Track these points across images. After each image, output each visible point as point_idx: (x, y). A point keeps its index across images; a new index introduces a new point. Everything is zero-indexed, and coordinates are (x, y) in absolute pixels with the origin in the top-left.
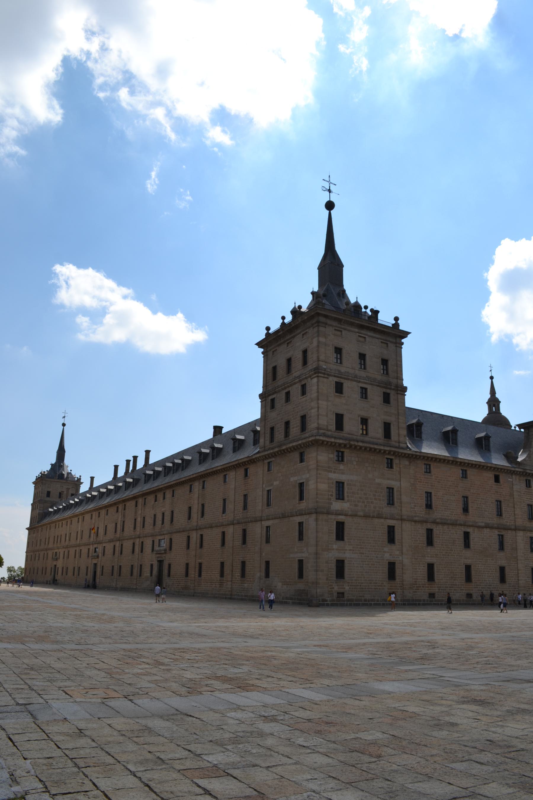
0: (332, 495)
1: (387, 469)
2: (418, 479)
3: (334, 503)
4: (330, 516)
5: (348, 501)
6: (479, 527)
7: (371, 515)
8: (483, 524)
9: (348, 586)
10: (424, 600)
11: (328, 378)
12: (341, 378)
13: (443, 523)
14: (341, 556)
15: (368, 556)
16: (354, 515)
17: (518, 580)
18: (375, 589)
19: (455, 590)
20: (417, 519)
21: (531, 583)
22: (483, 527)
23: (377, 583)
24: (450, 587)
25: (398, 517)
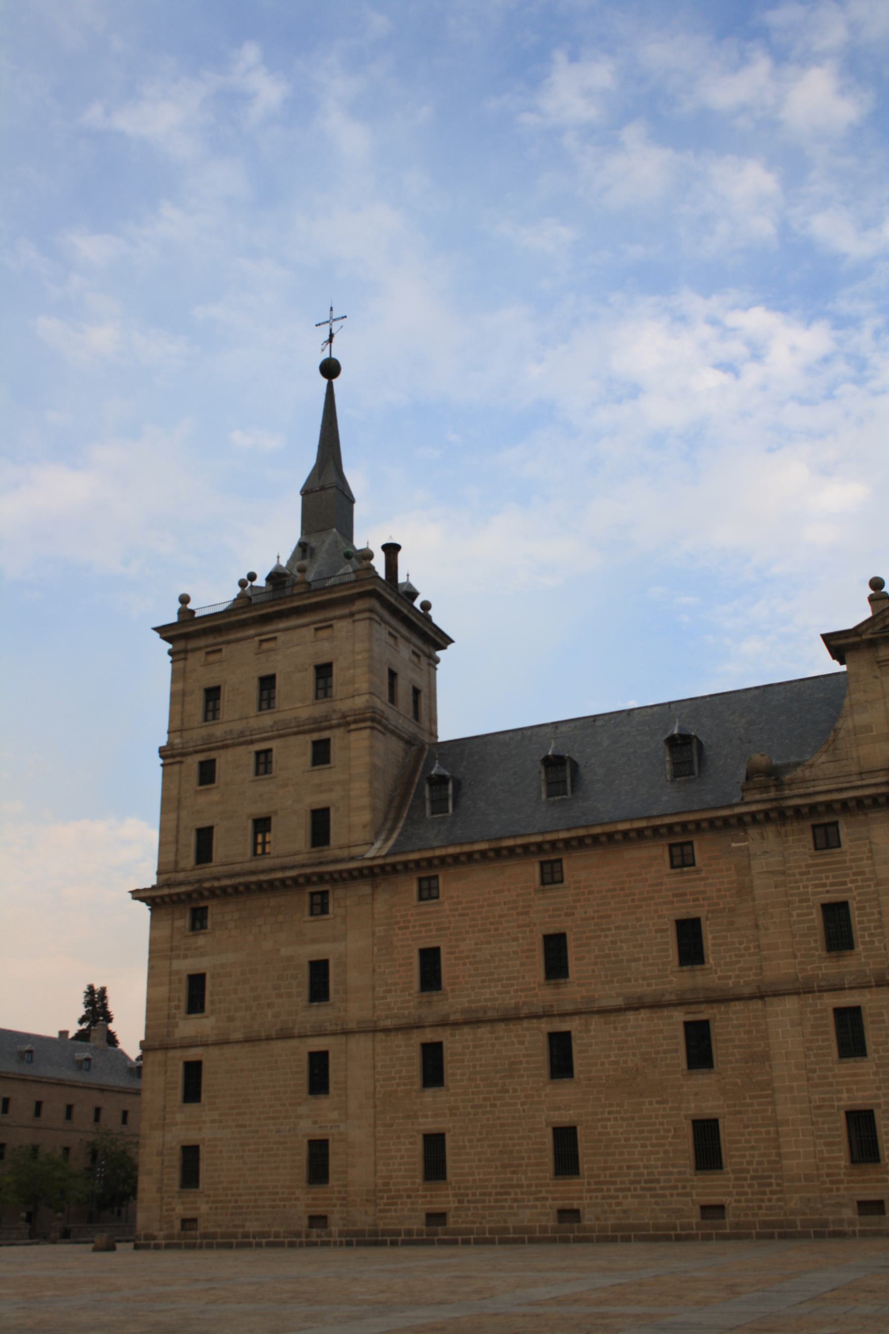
0: (177, 1007)
1: (312, 918)
2: (397, 923)
3: (181, 1023)
4: (171, 1053)
5: (212, 1012)
6: (604, 1012)
7: (263, 1035)
8: (620, 1002)
9: (207, 1202)
10: (409, 1232)
11: (181, 762)
12: (210, 750)
13: (474, 1020)
14: (191, 1137)
15: (257, 1132)
16: (223, 1042)
17: (779, 1155)
18: (273, 1207)
19: (515, 1200)
20: (388, 1023)
21: (843, 1163)
22: (619, 1010)
23: (277, 1193)
24: (498, 1194)
25: (334, 1028)
